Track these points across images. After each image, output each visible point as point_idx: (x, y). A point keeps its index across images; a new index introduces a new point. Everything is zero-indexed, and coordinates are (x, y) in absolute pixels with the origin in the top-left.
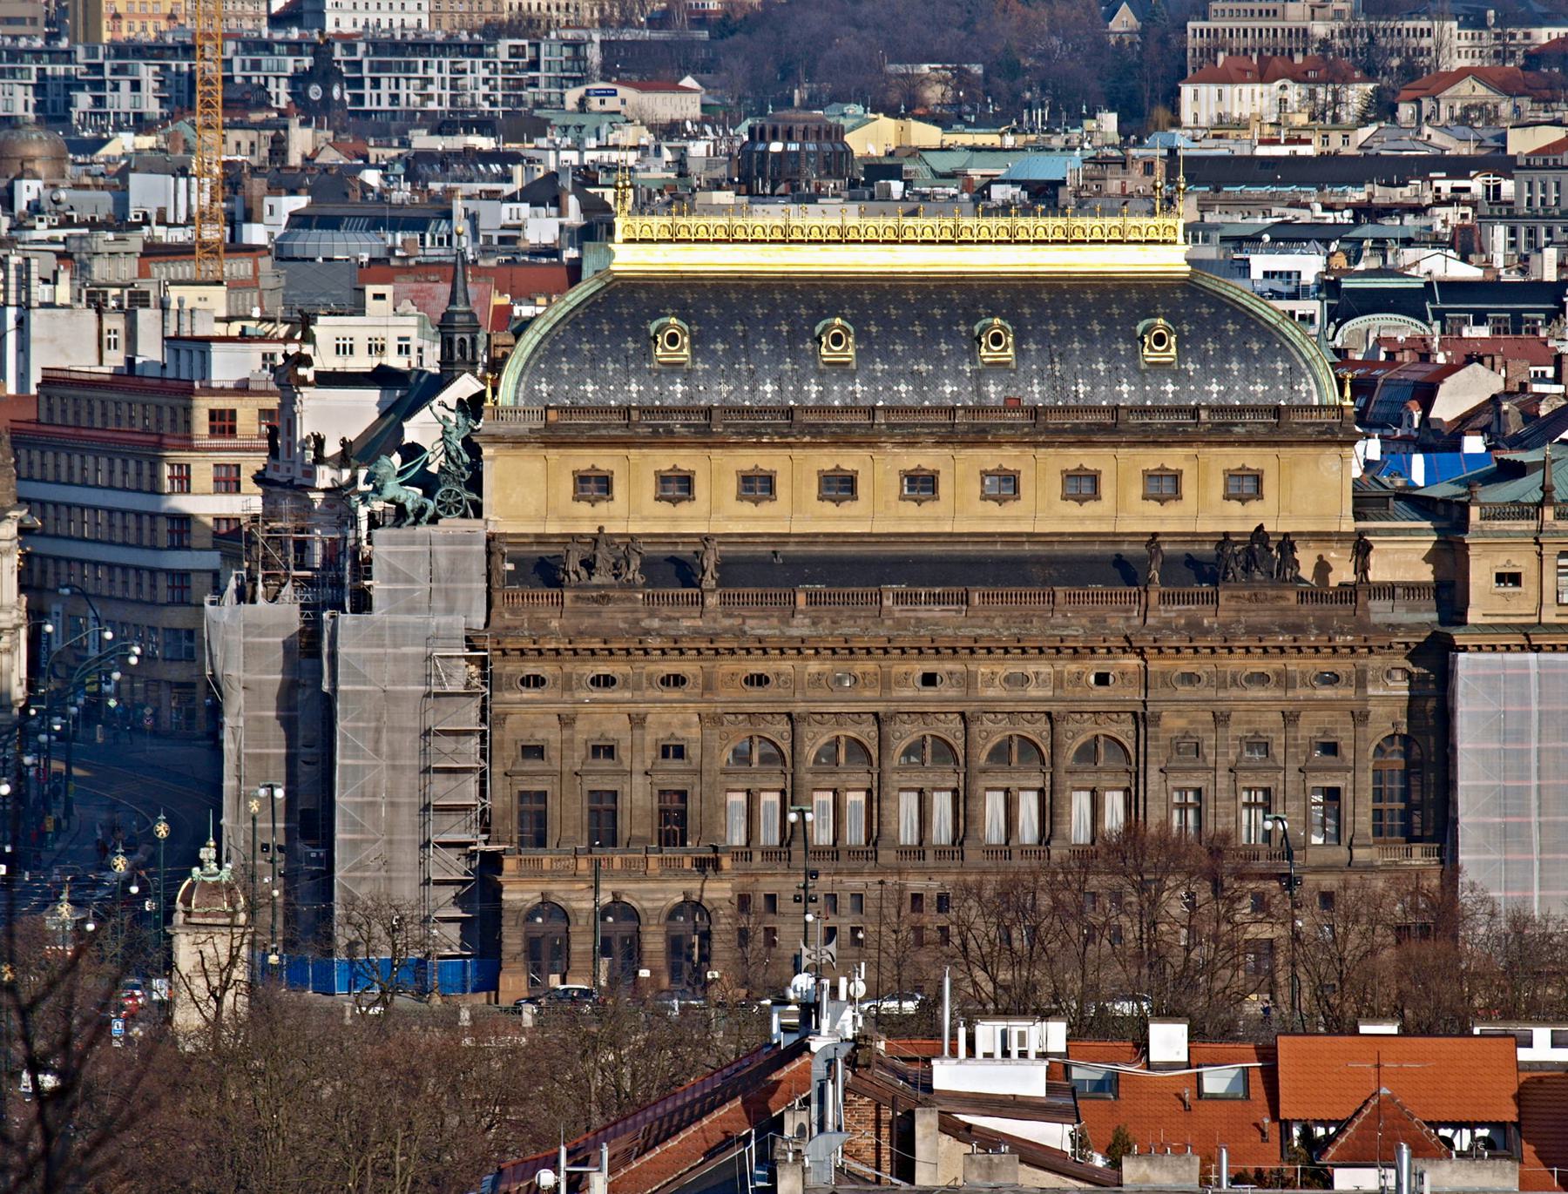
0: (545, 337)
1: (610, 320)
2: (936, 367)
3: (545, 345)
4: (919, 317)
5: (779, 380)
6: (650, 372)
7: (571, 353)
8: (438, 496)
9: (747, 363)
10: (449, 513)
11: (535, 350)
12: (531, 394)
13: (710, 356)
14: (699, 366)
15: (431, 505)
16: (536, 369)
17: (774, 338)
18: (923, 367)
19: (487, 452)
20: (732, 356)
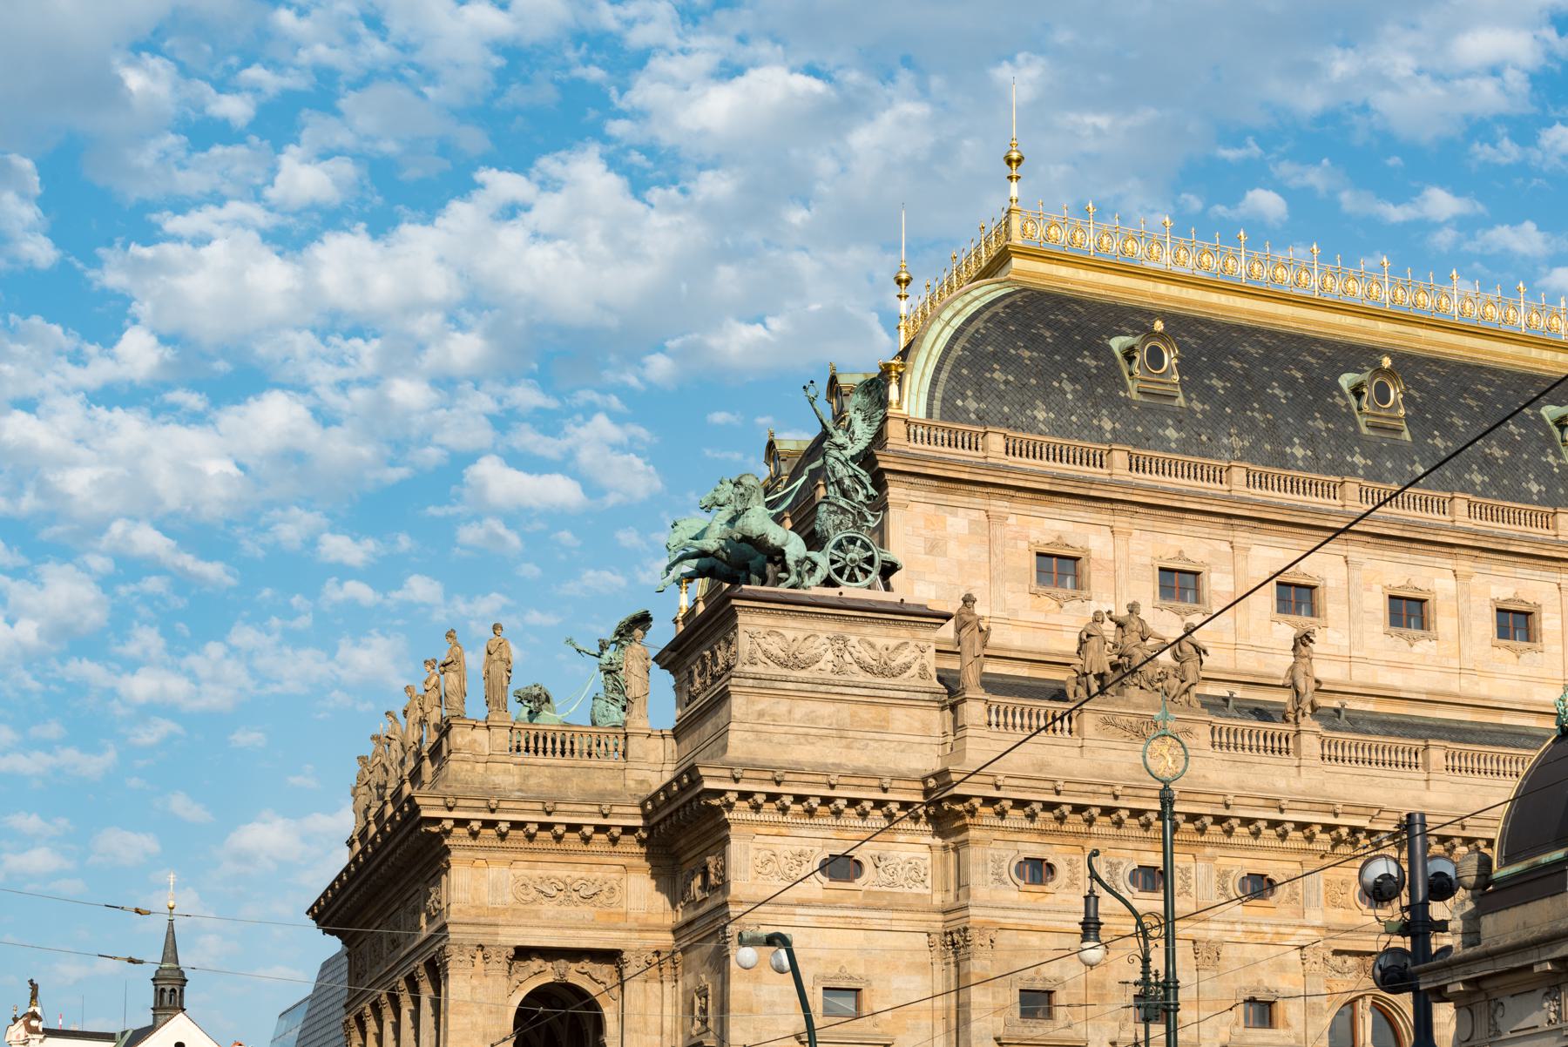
0: (959, 332)
1: (1048, 326)
2: (1513, 453)
3: (962, 341)
4: (1466, 390)
5: (1310, 441)
6: (1128, 402)
7: (1008, 362)
8: (830, 546)
9: (1263, 411)
10: (852, 578)
11: (948, 349)
12: (951, 412)
13: (1207, 394)
14: (1197, 406)
15: (822, 559)
16: (955, 375)
17: (1289, 384)
18: (1497, 452)
19: (896, 492)
20: (1241, 398)
